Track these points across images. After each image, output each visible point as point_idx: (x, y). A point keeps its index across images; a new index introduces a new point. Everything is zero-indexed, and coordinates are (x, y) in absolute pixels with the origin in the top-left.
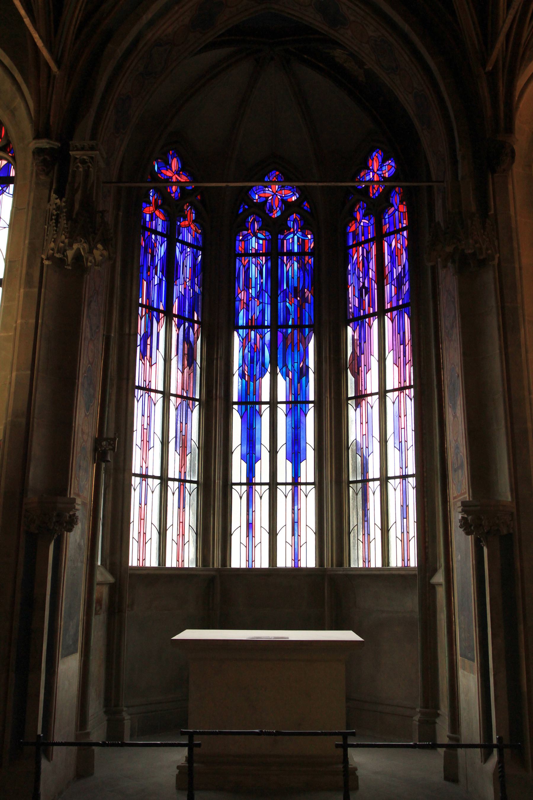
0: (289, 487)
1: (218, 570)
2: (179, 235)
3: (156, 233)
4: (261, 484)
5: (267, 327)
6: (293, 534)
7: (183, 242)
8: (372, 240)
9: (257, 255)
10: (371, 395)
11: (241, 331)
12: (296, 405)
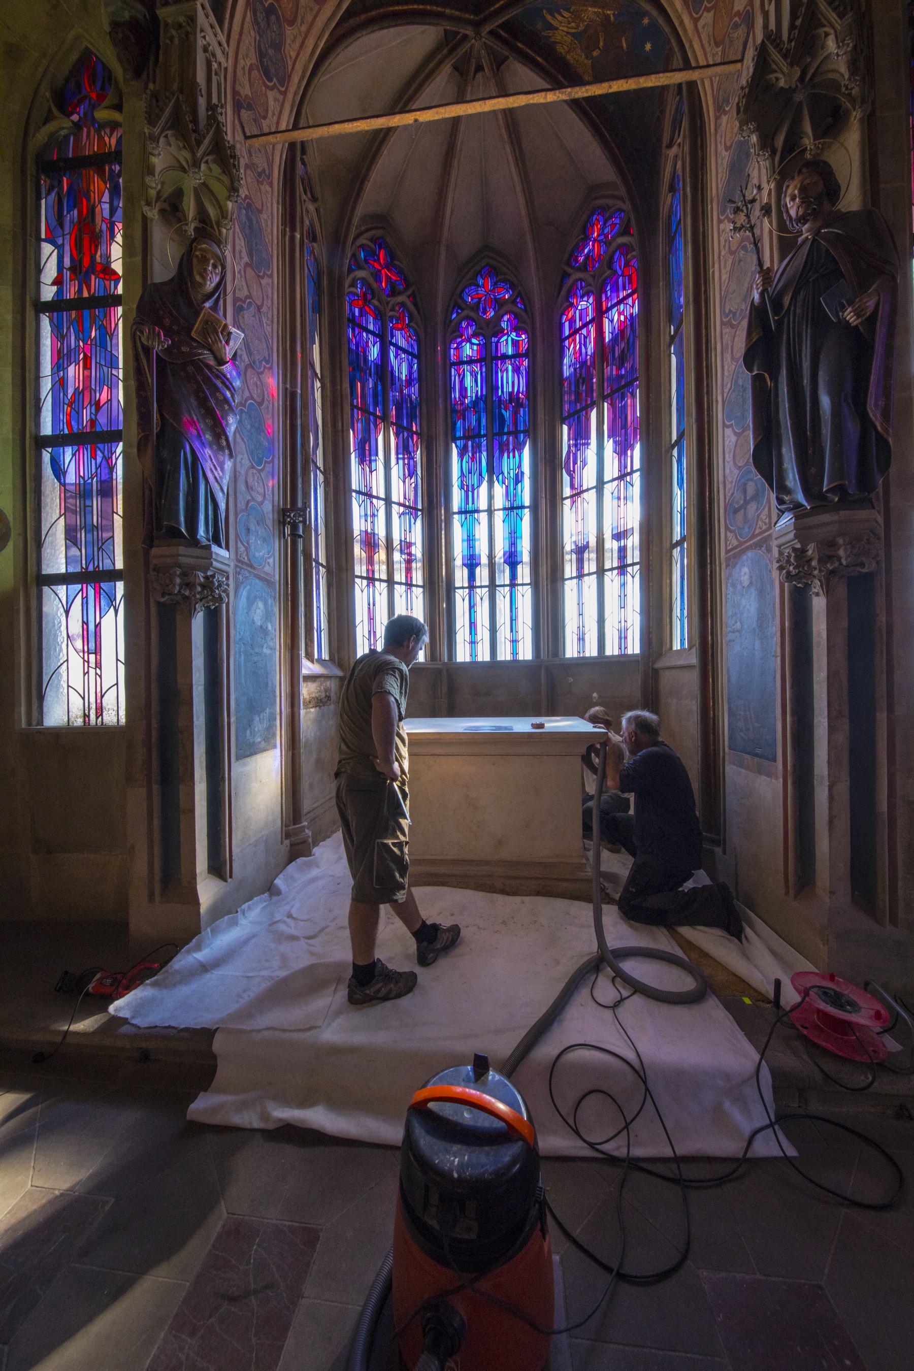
0: (507, 588)
1: (445, 664)
2: (392, 338)
3: (369, 332)
4: (481, 587)
5: (484, 436)
6: (512, 631)
7: (398, 348)
8: (591, 321)
9: (470, 362)
10: (587, 490)
11: (458, 442)
12: (512, 509)
